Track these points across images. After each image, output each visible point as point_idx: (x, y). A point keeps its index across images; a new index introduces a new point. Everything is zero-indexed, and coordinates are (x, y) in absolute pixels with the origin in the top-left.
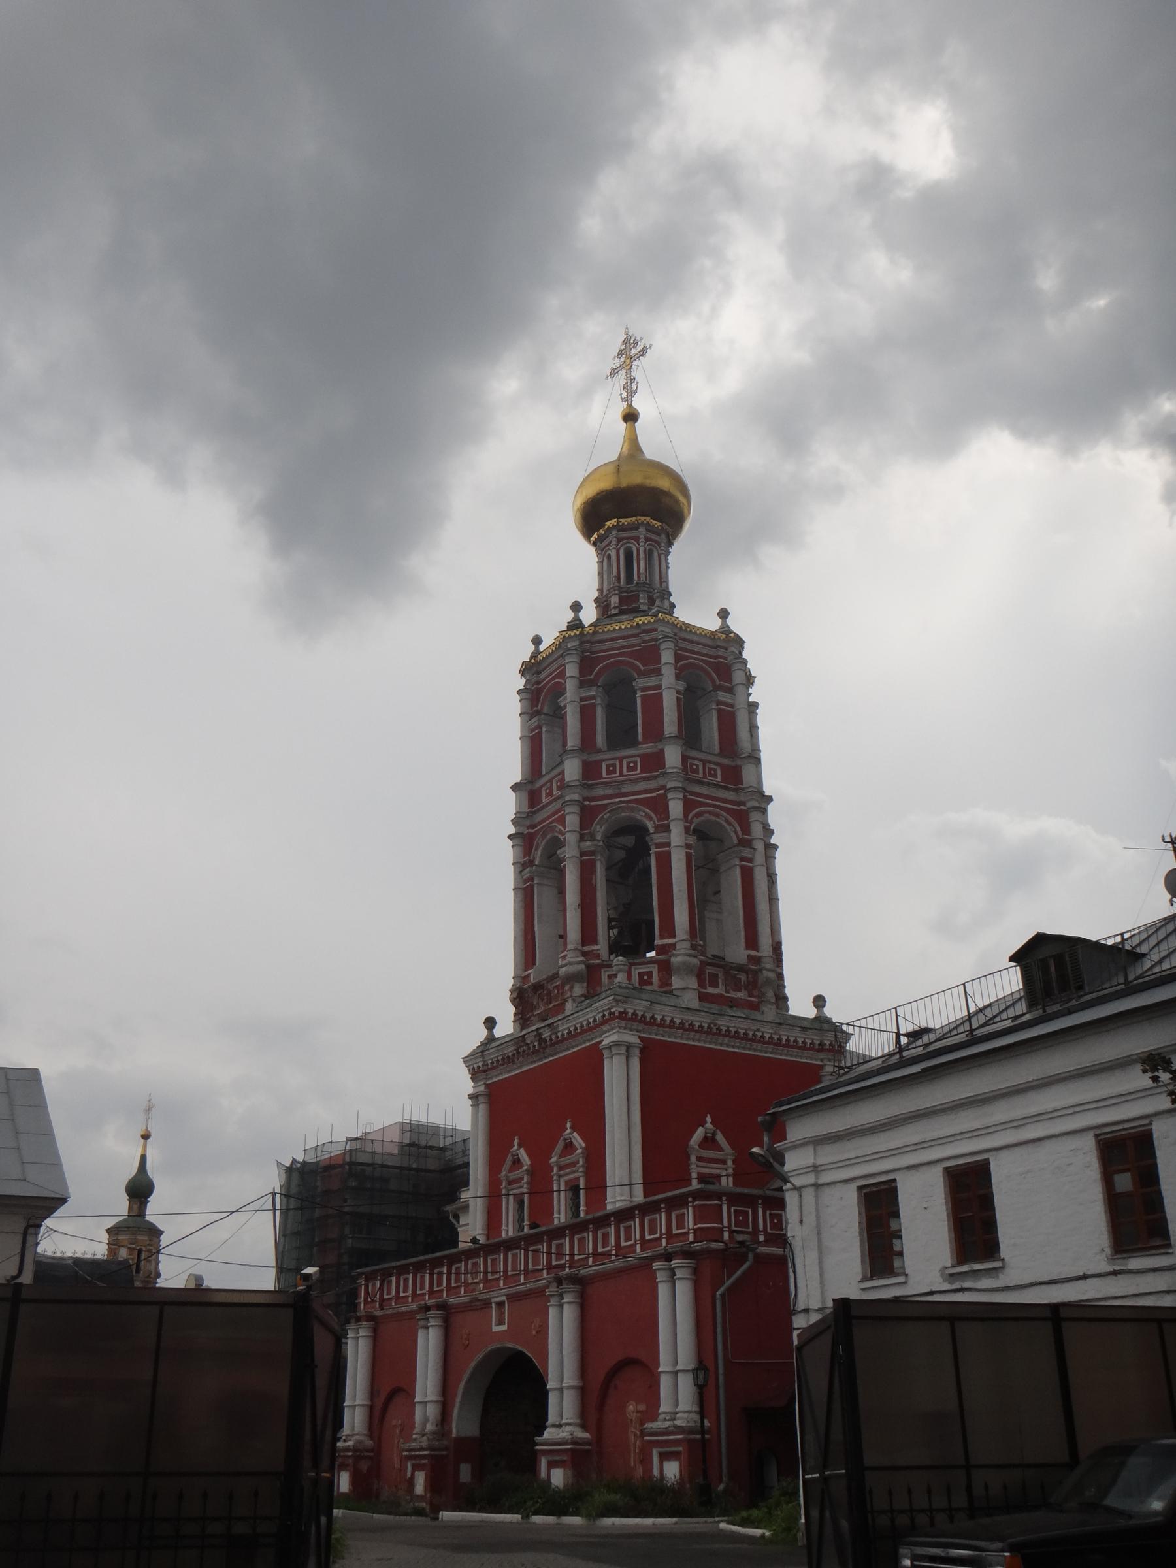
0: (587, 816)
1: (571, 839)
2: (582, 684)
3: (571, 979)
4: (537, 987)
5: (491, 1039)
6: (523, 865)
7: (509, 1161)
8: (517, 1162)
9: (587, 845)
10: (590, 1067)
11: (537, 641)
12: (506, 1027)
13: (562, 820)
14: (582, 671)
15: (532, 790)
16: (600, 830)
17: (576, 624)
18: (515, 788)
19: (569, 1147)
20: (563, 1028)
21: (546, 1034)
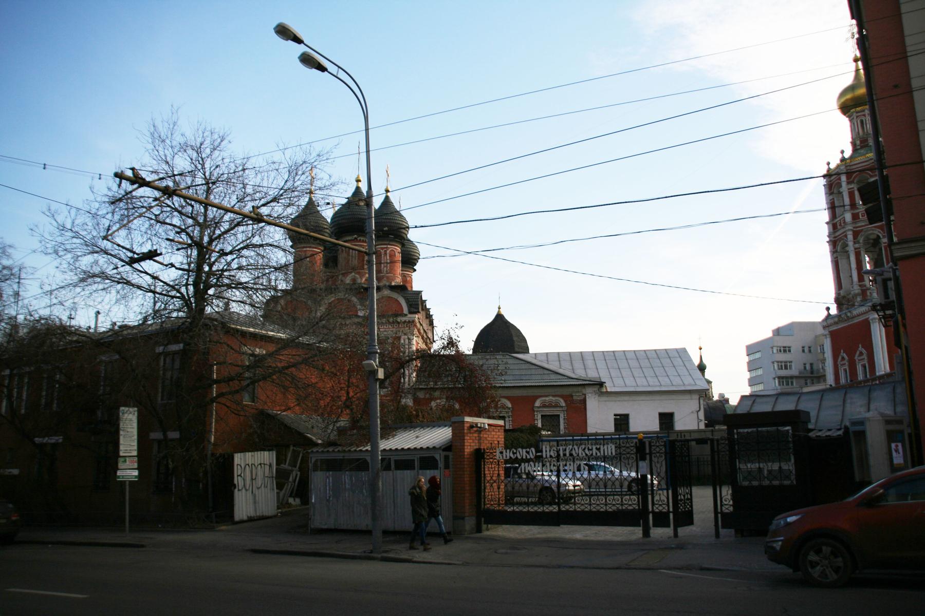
0: (856, 234)
1: (851, 244)
2: (848, 183)
3: (856, 295)
4: (844, 297)
5: (829, 315)
6: (834, 252)
7: (840, 358)
8: (843, 359)
9: (857, 246)
10: (865, 327)
11: (828, 164)
12: (834, 311)
13: (846, 236)
14: (848, 178)
15: (835, 225)
16: (861, 239)
17: (843, 160)
18: (827, 223)
19: (861, 354)
20: (855, 312)
21: (849, 314)
